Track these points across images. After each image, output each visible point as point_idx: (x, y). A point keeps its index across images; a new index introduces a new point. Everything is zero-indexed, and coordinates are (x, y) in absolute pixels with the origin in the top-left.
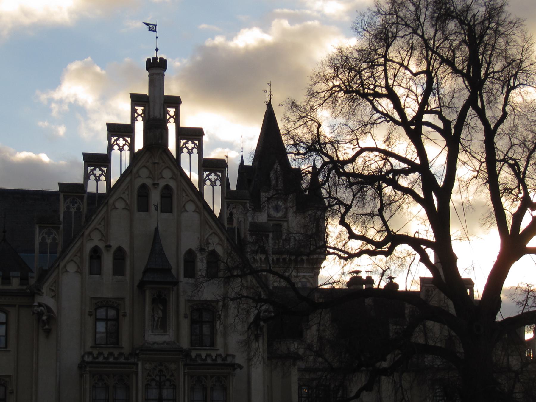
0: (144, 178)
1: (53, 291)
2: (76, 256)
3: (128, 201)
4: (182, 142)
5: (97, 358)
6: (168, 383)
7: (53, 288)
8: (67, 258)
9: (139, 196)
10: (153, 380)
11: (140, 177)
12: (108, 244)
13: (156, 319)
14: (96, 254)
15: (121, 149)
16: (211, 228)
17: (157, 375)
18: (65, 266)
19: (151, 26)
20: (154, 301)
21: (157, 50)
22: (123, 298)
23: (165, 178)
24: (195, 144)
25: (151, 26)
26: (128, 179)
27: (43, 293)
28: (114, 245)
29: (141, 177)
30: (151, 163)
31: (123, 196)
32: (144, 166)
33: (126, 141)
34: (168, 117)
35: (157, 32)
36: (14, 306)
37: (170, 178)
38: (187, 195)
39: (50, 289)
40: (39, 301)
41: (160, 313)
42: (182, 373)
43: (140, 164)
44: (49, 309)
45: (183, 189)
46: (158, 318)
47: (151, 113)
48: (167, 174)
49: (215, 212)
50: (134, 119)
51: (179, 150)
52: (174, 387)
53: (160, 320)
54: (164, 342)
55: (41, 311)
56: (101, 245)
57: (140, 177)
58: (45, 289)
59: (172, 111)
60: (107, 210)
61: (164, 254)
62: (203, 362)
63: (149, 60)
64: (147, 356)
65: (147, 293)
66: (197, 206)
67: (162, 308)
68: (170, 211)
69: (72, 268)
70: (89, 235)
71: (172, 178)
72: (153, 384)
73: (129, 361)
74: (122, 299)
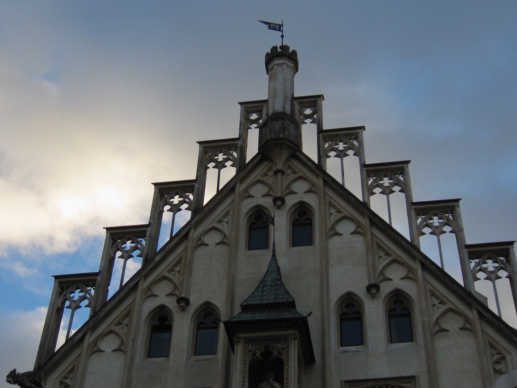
2: (119, 323)
3: (226, 232)
7: (68, 381)
11: (251, 196)
16: (387, 254)
18: (95, 343)
19: (272, 25)
23: (296, 193)
25: (272, 25)
26: (228, 201)
29: (254, 197)
30: (271, 176)
32: (259, 182)
35: (282, 31)
37: (306, 192)
38: (339, 212)
39: (61, 383)
45: (331, 205)
48: (300, 187)
51: (322, 155)
56: (171, 303)
57: (251, 196)
59: (308, 111)
60: (186, 247)
61: (282, 284)
63: (267, 55)
65: (239, 348)
66: (359, 225)
68: (310, 242)
70: (149, 288)
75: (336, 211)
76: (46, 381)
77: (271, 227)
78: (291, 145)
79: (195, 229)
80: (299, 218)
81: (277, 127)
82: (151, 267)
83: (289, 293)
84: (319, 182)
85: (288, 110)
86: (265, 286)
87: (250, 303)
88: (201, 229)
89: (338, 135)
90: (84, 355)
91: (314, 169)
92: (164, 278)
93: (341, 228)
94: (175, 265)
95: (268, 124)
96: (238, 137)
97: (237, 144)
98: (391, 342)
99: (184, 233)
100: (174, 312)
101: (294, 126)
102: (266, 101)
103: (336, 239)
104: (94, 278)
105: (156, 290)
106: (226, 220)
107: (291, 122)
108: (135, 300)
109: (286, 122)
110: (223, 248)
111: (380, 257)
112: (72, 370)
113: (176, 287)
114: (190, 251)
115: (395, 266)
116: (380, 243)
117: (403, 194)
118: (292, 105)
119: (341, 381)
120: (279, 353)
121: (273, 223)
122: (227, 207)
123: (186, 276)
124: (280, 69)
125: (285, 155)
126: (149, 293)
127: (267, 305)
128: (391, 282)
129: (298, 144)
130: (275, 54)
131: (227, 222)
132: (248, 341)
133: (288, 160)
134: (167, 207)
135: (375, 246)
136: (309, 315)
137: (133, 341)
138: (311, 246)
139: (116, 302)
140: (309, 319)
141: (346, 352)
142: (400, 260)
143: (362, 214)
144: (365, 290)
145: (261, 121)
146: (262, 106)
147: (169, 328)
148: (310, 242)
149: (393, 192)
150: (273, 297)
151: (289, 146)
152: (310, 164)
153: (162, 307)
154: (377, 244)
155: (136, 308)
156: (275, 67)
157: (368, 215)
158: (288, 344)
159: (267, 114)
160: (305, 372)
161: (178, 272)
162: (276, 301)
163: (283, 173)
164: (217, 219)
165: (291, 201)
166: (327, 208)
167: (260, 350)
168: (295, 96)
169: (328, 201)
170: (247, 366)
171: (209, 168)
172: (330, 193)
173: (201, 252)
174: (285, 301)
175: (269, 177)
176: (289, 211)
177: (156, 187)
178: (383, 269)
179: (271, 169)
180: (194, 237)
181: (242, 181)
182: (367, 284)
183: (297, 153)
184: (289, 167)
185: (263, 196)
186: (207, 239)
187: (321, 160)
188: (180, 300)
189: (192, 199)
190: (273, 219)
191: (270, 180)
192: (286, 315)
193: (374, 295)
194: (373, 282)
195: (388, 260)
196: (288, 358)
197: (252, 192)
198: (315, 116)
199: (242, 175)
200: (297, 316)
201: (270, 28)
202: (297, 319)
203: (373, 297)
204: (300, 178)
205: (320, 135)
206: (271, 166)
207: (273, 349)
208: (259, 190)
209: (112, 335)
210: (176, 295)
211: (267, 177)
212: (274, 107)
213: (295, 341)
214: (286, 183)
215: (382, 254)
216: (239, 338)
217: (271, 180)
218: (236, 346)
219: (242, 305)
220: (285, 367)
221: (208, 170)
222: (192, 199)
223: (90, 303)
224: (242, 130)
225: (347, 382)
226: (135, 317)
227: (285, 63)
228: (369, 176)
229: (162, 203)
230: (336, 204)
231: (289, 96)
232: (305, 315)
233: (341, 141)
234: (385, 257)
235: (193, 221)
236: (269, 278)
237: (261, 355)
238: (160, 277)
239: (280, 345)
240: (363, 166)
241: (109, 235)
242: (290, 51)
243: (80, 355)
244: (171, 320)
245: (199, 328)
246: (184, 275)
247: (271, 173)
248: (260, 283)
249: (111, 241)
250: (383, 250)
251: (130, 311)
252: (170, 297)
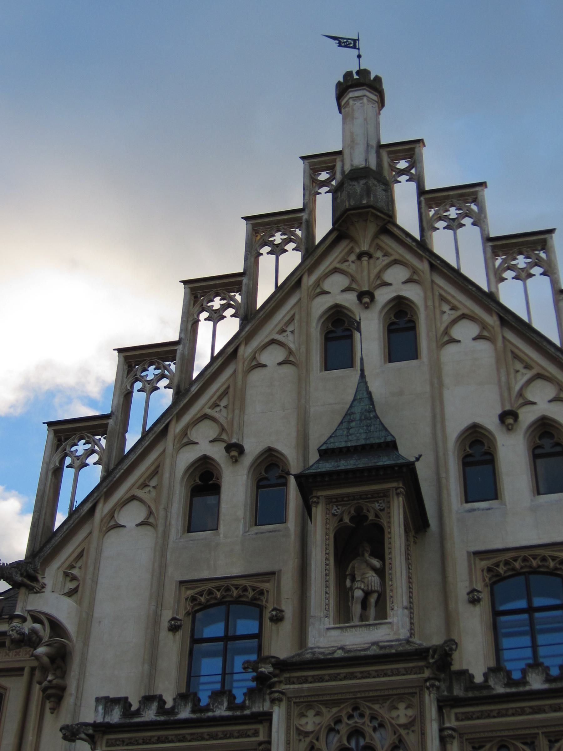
1: (74, 578)
2: (144, 485)
3: (292, 346)
5: (138, 713)
7: (75, 572)
12: (234, 441)
13: (358, 594)
16: (527, 367)
18: (112, 515)
19: (343, 41)
22: (273, 573)
23: (390, 284)
25: (343, 41)
26: (293, 301)
27: (43, 586)
29: (329, 293)
30: (353, 262)
32: (336, 270)
35: (359, 49)
38: (454, 308)
39: (66, 575)
40: (29, 608)
41: (373, 579)
42: (432, 729)
45: (443, 299)
46: (367, 594)
49: (536, 325)
53: (373, 599)
54: (373, 644)
55: (33, 631)
59: (402, 165)
60: (235, 371)
61: (376, 417)
62: (514, 690)
63: (339, 84)
64: (305, 686)
65: (319, 512)
66: (484, 326)
67: (376, 563)
68: (414, 354)
70: (184, 433)
71: (409, 281)
73: (247, 712)
74: (271, 575)
75: (449, 307)
76: (43, 574)
77: (357, 335)
78: (379, 214)
79: (246, 344)
80: (395, 320)
81: (358, 190)
82: (185, 402)
83: (386, 430)
84: (424, 267)
85: (373, 164)
86: (352, 421)
87: (331, 446)
88: (256, 343)
89: (448, 197)
90: (96, 533)
91: (416, 249)
92: (206, 417)
93: (457, 332)
94: (221, 398)
95: (345, 186)
96: (301, 207)
97: (300, 219)
98: (539, 494)
99: (230, 350)
100: (223, 466)
101: (384, 187)
102: (340, 153)
103: (452, 348)
104: (105, 422)
105: (195, 434)
106: (290, 328)
107: (379, 181)
108: (164, 451)
109: (372, 182)
110: (288, 370)
111: (517, 371)
112: (81, 555)
113: (223, 429)
114: (240, 376)
115: (539, 383)
116: (516, 351)
117: (547, 279)
118: (379, 157)
119: (468, 553)
120: (377, 516)
121: (359, 330)
122: (291, 309)
123: (237, 412)
124: (358, 104)
125: (372, 229)
126: (185, 440)
127: (356, 447)
128: (534, 407)
129: (390, 213)
130: (350, 83)
131: (292, 332)
132: (330, 500)
133: (376, 236)
134: (204, 315)
135: (509, 355)
136: (418, 459)
137: (166, 509)
138: (416, 360)
139: (137, 454)
140: (418, 465)
141: (473, 510)
142: (547, 374)
143: (489, 310)
144: (497, 421)
145: (334, 183)
146: (335, 161)
147: (216, 489)
148: (414, 354)
149: (531, 275)
150: (363, 436)
151: (377, 217)
152: (408, 240)
153: (205, 460)
154: (512, 352)
155: (168, 462)
156: (351, 102)
157: (496, 310)
158: (389, 502)
159: (343, 172)
160: (415, 542)
161: (225, 407)
162: (368, 442)
163: (370, 256)
164: (278, 328)
166: (437, 304)
167: (349, 513)
168: (382, 143)
169: (437, 294)
170: (332, 536)
171: (262, 254)
172: (440, 281)
173: (256, 376)
174: (382, 440)
175: (350, 262)
176: (381, 312)
177: (187, 286)
178: (521, 389)
179: (353, 252)
180: (247, 354)
181: (311, 271)
182: (499, 411)
183: (390, 227)
184: (379, 247)
185: (343, 291)
186: (264, 358)
187: (425, 234)
188: (229, 448)
189: (240, 301)
190: (359, 323)
191: (352, 268)
192: (385, 461)
193: (510, 427)
194: (508, 408)
195: (529, 375)
196: (389, 522)
197: (327, 285)
198: (413, 171)
199: (309, 262)
200: (401, 461)
201: (340, 45)
202: (401, 466)
203: (509, 429)
204: (396, 262)
205: (422, 199)
206: (352, 247)
207: (368, 511)
209: (135, 503)
210: (223, 441)
211: (346, 264)
212: (352, 161)
213: (398, 497)
214: (375, 271)
215: (519, 366)
216: (318, 497)
217: (353, 266)
218: (314, 509)
219: (319, 451)
220: (387, 536)
221: (261, 258)
222: (240, 301)
223: (100, 459)
224: (307, 197)
225: (476, 553)
226: (166, 475)
227: (365, 96)
228: (495, 254)
229: (197, 308)
230: (449, 298)
231: (374, 143)
232: (412, 459)
233: (452, 206)
234: (525, 371)
235: (243, 333)
236: (357, 409)
237: (351, 520)
238: (199, 415)
239: (377, 505)
240: (487, 239)
241: (122, 359)
242: (372, 77)
243: (90, 533)
244: (219, 477)
245: (259, 487)
246: (233, 411)
247: (353, 257)
248: (344, 417)
249: (126, 367)
250: (521, 360)
251: (158, 466)
252: (216, 444)
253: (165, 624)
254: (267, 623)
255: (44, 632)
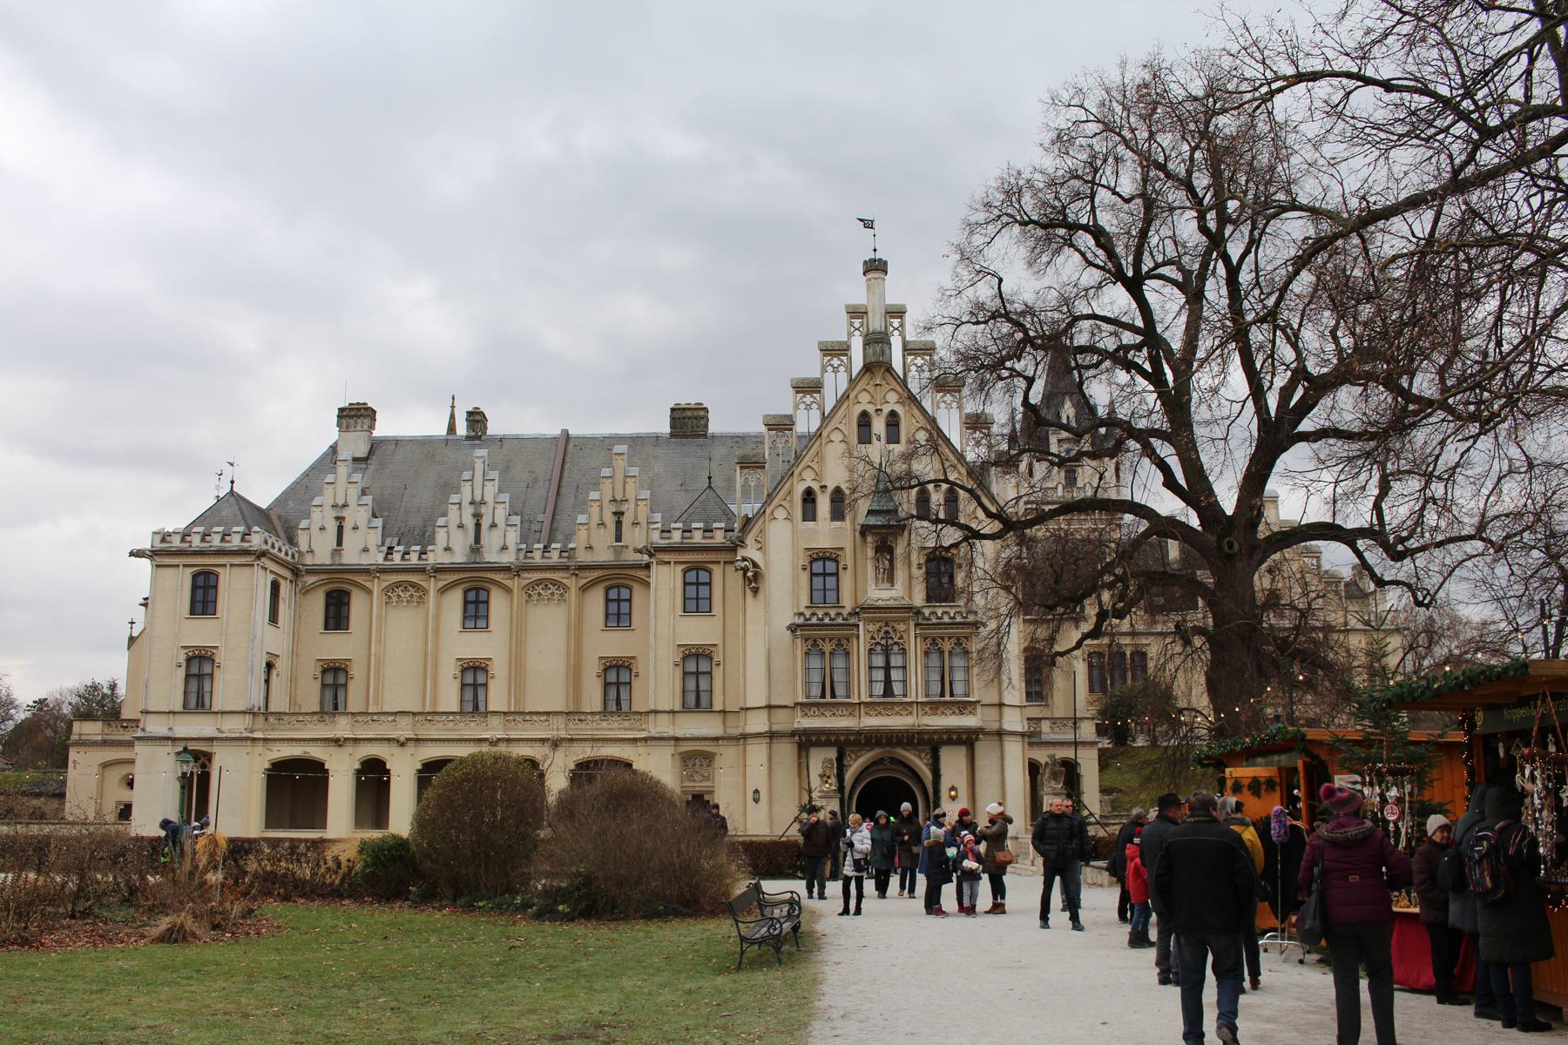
0: (864, 403)
4: (910, 358)
5: (809, 619)
6: (896, 648)
8: (775, 503)
9: (859, 426)
10: (878, 643)
13: (882, 570)
14: (809, 497)
15: (835, 369)
17: (882, 638)
20: (878, 550)
21: (875, 250)
24: (926, 361)
28: (831, 488)
31: (839, 426)
32: (864, 389)
33: (842, 361)
34: (892, 329)
36: (719, 562)
41: (887, 562)
43: (859, 388)
44: (755, 565)
47: (870, 326)
50: (850, 335)
52: (904, 651)
56: (815, 486)
58: (750, 540)
59: (896, 322)
63: (865, 262)
65: (869, 539)
69: (781, 514)
72: (879, 648)
74: (841, 549)
105: (804, 475)
125: (882, 370)
132: (873, 534)
147: (814, 501)
165: (887, 409)
186: (833, 437)
208: (864, 397)
253: (800, 567)
254: (840, 569)
255: (751, 566)
